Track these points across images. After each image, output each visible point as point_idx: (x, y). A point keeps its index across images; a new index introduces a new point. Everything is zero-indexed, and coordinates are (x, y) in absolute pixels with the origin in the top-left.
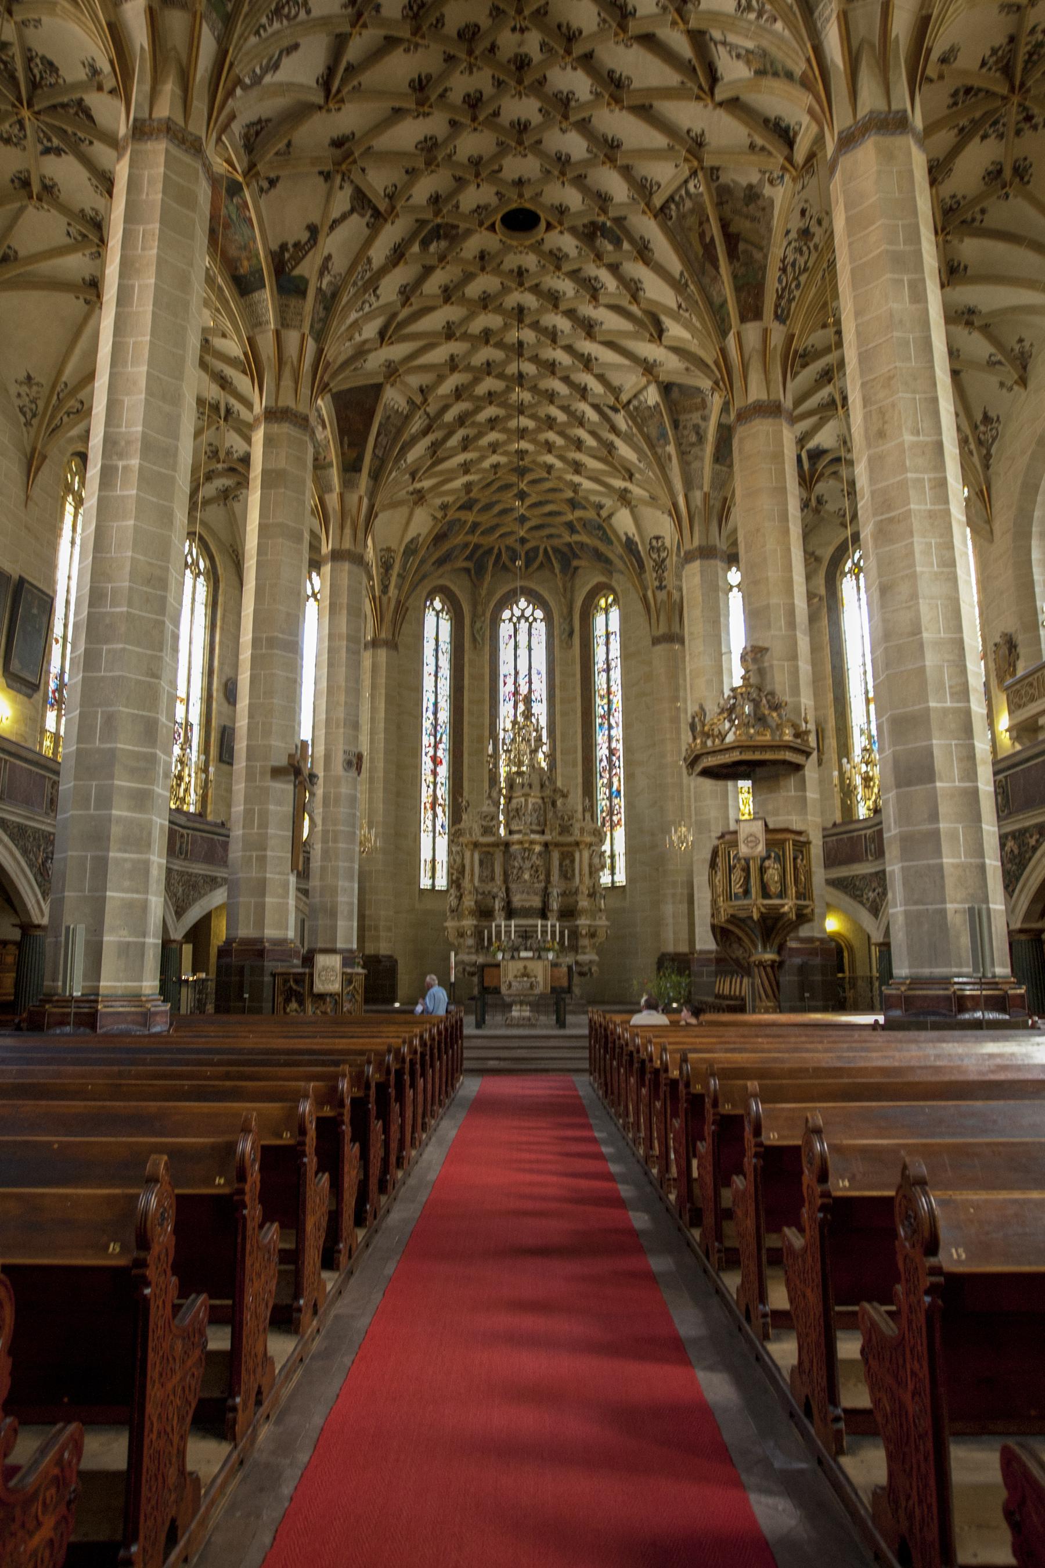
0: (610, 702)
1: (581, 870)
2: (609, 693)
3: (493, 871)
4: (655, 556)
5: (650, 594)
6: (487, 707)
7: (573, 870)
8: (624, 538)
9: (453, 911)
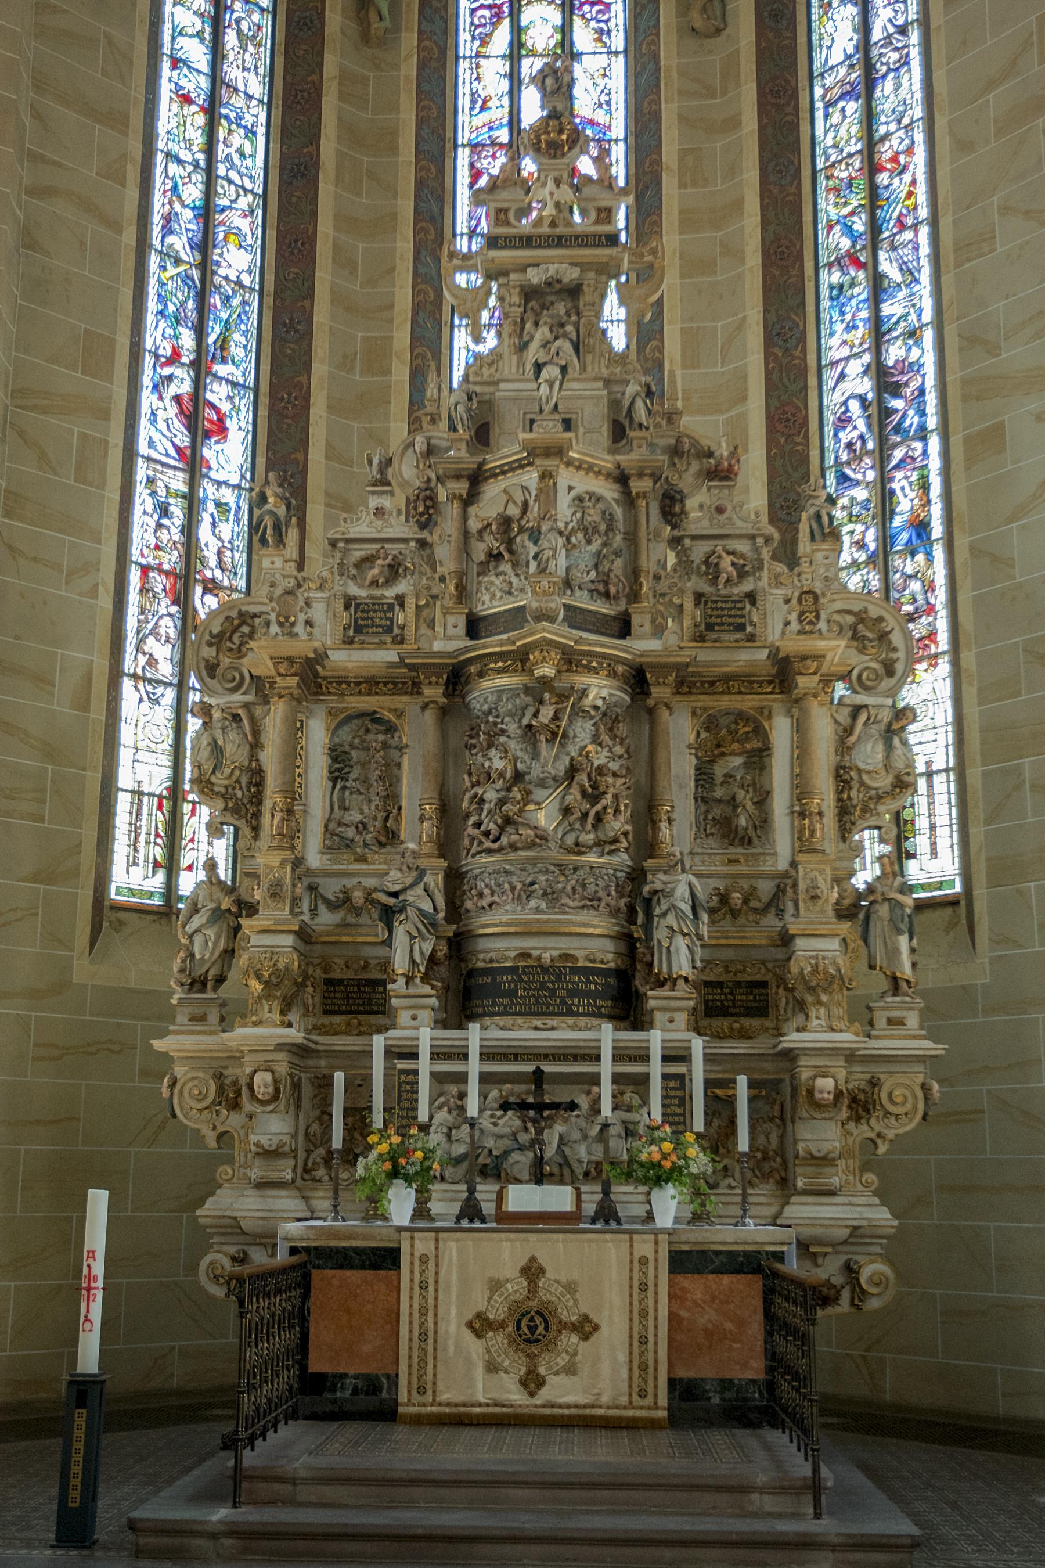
1: (801, 791)
2: (873, 168)
3: (391, 798)
6: (404, 244)
7: (763, 800)
9: (198, 984)
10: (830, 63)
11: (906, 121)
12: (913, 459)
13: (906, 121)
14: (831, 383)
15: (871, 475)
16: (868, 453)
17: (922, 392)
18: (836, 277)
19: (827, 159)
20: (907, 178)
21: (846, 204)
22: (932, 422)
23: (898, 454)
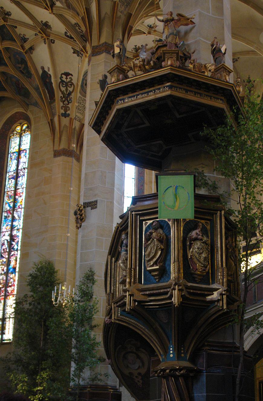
0: (15, 201)
2: (15, 194)
4: (63, 89)
5: (56, 119)
10: (11, 170)
11: (22, 187)
12: (15, 255)
13: (22, 187)
14: (2, 236)
15: (7, 256)
16: (7, 252)
17: (18, 241)
18: (6, 214)
19: (7, 190)
20: (21, 198)
21: (10, 200)
22: (19, 248)
23: (12, 253)
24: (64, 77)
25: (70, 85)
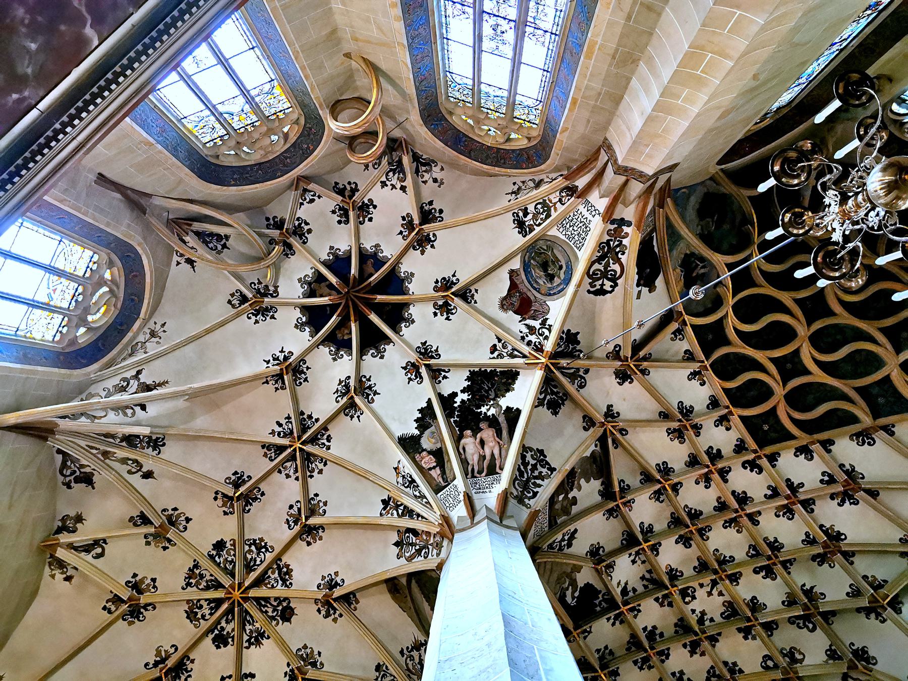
8: (659, 282)
24: (607, 287)
25: (597, 274)
